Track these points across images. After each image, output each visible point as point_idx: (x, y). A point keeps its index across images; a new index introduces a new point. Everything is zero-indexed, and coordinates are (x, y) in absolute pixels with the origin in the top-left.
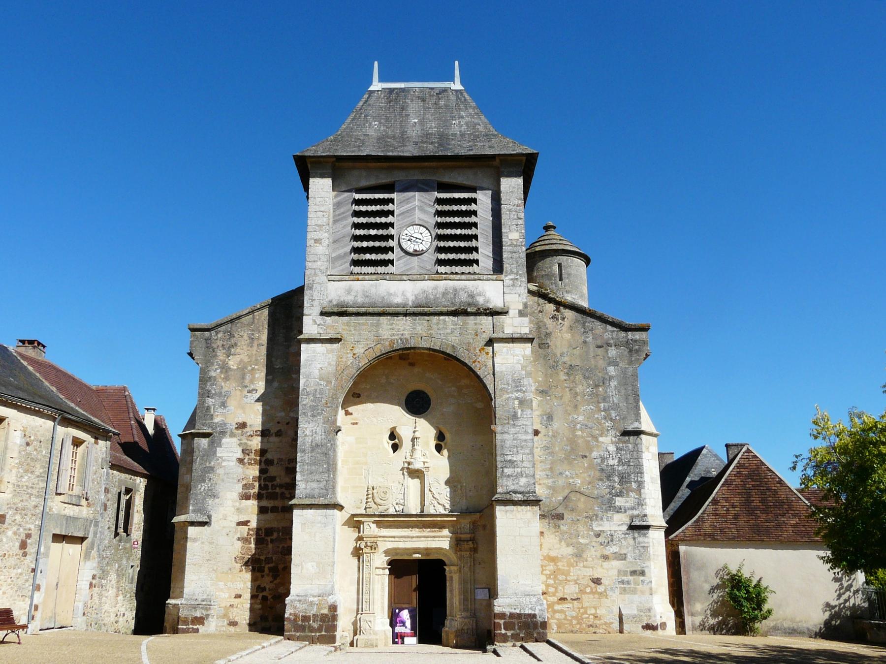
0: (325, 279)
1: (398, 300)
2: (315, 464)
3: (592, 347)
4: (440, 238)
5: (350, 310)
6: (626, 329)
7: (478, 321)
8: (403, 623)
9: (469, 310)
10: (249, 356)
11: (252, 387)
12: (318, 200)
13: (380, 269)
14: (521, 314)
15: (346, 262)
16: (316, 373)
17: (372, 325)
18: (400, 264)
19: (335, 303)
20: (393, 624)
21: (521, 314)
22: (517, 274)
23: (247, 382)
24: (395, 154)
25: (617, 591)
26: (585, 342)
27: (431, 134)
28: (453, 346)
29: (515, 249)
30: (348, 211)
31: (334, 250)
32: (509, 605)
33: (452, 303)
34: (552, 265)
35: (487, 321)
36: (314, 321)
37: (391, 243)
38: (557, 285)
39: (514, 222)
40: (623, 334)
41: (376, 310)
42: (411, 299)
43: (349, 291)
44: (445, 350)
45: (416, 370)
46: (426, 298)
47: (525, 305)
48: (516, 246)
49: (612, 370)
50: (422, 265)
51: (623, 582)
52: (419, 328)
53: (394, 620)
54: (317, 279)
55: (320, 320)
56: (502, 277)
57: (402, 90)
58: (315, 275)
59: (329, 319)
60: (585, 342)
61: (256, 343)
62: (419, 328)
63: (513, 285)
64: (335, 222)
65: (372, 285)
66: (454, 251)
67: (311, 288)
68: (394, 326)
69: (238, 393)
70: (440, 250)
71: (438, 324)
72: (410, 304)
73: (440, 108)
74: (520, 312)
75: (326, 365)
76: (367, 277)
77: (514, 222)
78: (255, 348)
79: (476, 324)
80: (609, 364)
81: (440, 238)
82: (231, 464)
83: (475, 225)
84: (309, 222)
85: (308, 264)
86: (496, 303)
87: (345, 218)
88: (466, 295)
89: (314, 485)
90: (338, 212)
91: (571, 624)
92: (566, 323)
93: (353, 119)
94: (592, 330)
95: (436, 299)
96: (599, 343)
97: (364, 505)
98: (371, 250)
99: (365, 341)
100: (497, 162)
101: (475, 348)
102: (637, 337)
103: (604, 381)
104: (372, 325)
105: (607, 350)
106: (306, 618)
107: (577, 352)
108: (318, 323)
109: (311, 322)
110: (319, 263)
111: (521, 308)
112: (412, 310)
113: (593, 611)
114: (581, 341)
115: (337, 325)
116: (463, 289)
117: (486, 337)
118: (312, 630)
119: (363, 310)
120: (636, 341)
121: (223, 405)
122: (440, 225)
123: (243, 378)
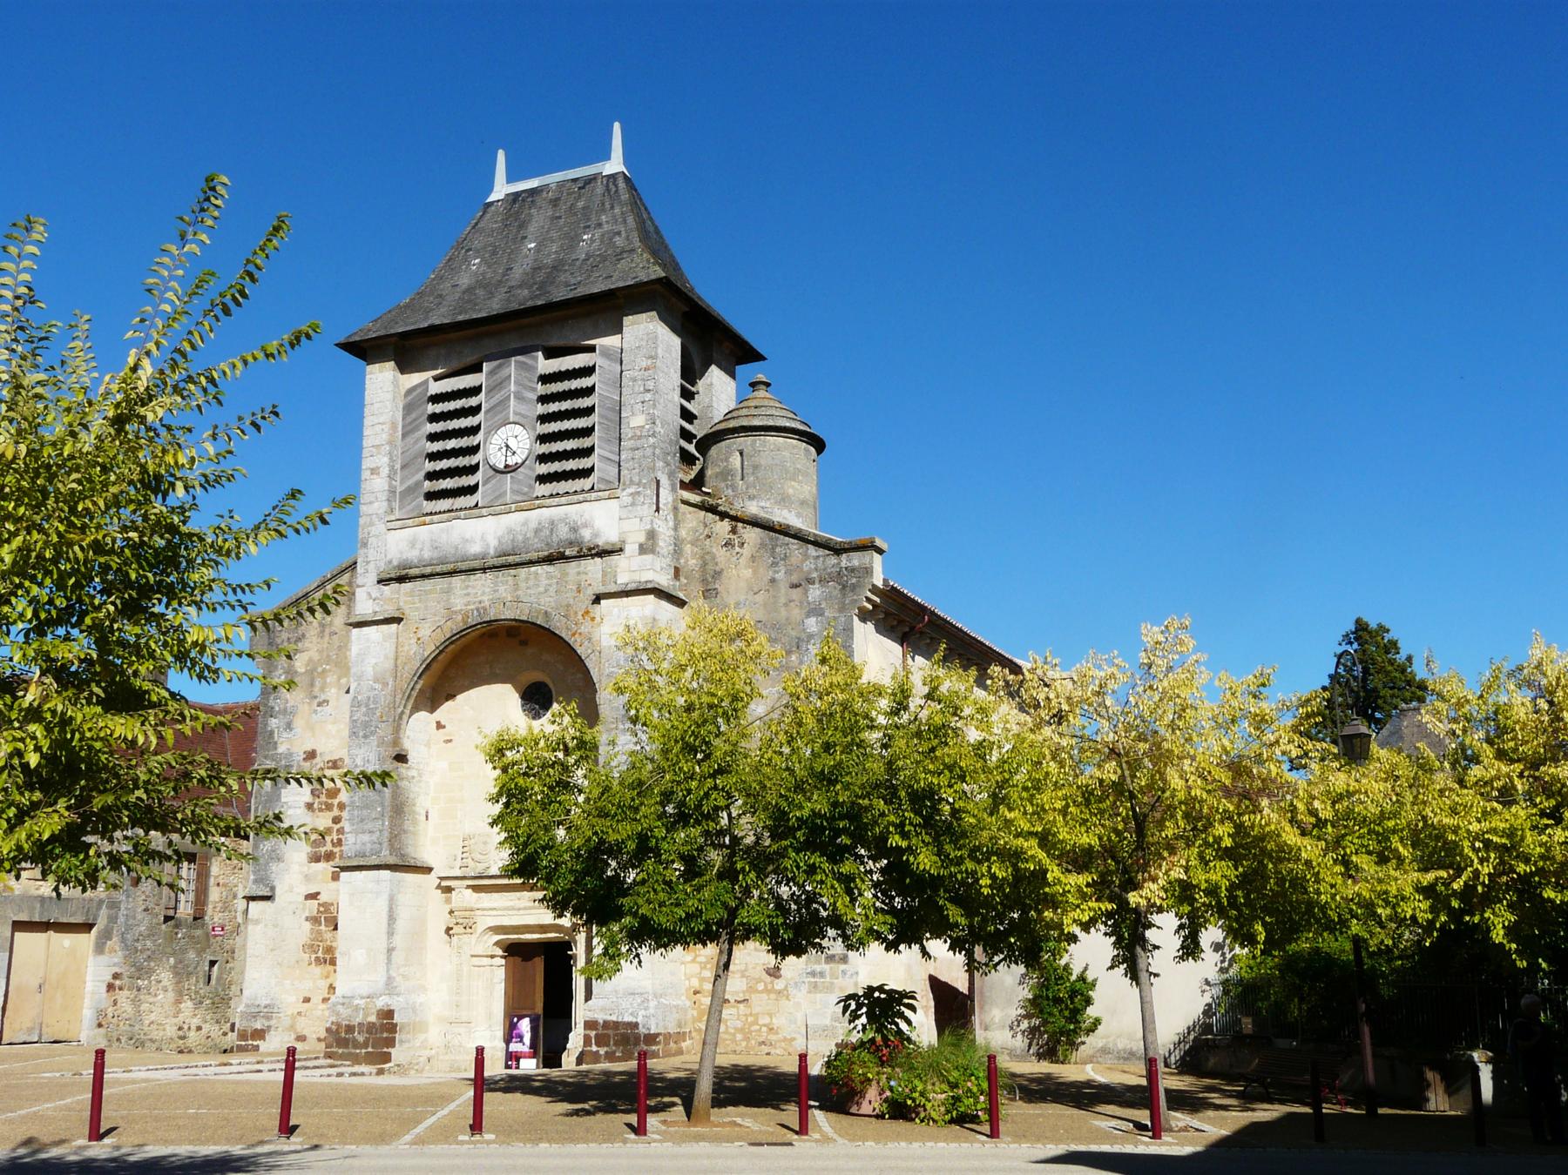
0: (382, 527)
1: (475, 549)
2: (366, 807)
3: (783, 587)
4: (544, 439)
6: (838, 550)
8: (521, 1037)
10: (320, 652)
11: (323, 697)
16: (370, 671)
17: (443, 591)
19: (395, 563)
20: (508, 1041)
23: (316, 690)
24: (467, 317)
25: (805, 988)
26: (773, 581)
32: (603, 1009)
34: (727, 455)
35: (594, 566)
38: (734, 487)
40: (833, 560)
41: (445, 568)
42: (492, 545)
43: (413, 544)
45: (530, 651)
48: (640, 438)
49: (812, 624)
51: (813, 974)
52: (502, 589)
53: (511, 1034)
55: (378, 590)
57: (533, 192)
58: (372, 524)
59: (387, 590)
60: (773, 581)
62: (502, 589)
63: (633, 504)
64: (404, 436)
66: (565, 459)
69: (306, 707)
71: (527, 579)
72: (492, 552)
74: (641, 546)
76: (435, 518)
78: (327, 638)
82: (299, 811)
85: (363, 508)
87: (417, 428)
88: (566, 529)
89: (366, 838)
90: (409, 419)
91: (734, 1041)
92: (746, 551)
94: (785, 557)
96: (795, 579)
97: (459, 863)
98: (450, 474)
102: (856, 563)
103: (798, 645)
104: (443, 591)
105: (806, 591)
106: (350, 1029)
107: (759, 598)
109: (364, 596)
111: (642, 539)
112: (491, 562)
113: (766, 1020)
117: (590, 593)
118: (356, 1045)
119: (428, 570)
120: (852, 570)
121: (289, 726)
123: (312, 685)
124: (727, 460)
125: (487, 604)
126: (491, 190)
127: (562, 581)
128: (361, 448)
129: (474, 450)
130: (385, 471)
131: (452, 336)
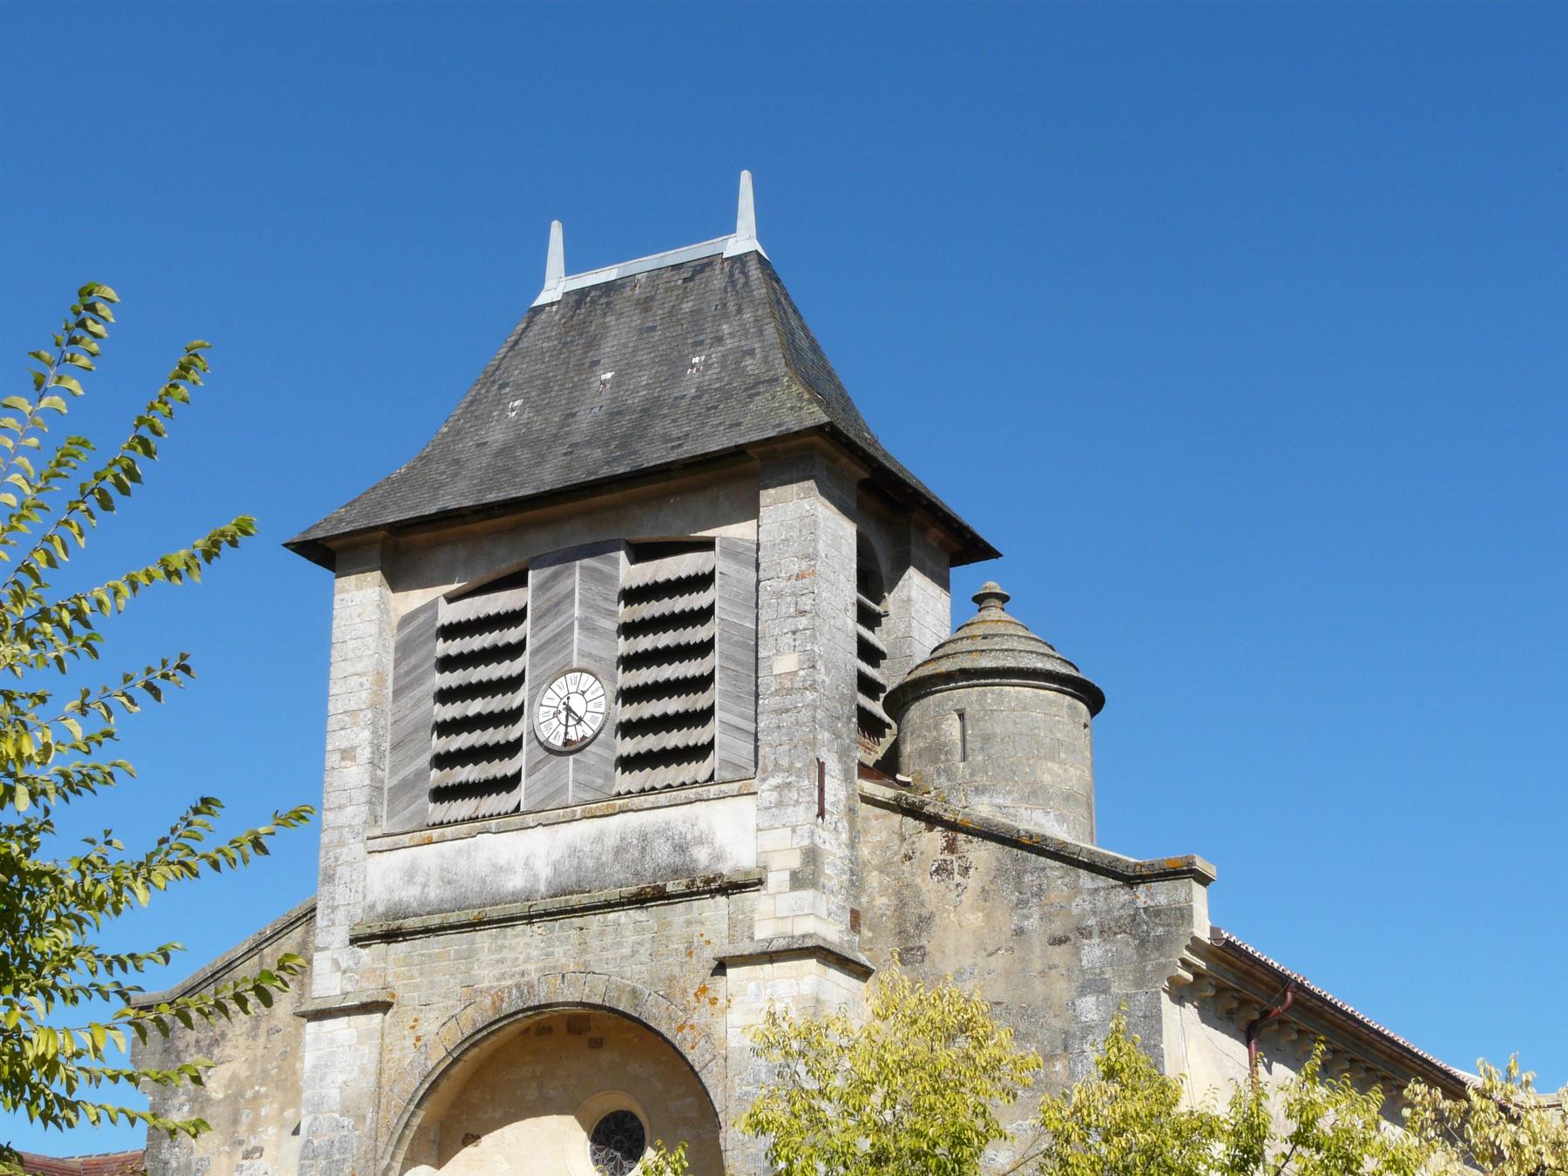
1: (515, 882)
3: (1038, 942)
4: (629, 696)
5: (411, 923)
6: (1131, 879)
7: (694, 915)
9: (670, 888)
10: (251, 1063)
11: (253, 1142)
12: (351, 644)
15: (417, 797)
16: (334, 1095)
17: (459, 956)
19: (380, 909)
22: (789, 771)
23: (242, 1130)
26: (1020, 932)
28: (634, 991)
29: (788, 701)
30: (426, 659)
33: (637, 873)
34: (937, 719)
36: (336, 962)
38: (949, 773)
40: (1122, 895)
43: (410, 875)
44: (613, 1004)
45: (606, 1057)
46: (578, 867)
48: (790, 691)
49: (1089, 1007)
52: (559, 951)
57: (608, 288)
58: (342, 843)
59: (365, 954)
60: (1020, 932)
61: (264, 1027)
63: (780, 804)
64: (397, 693)
65: (460, 851)
66: (665, 729)
68: (505, 953)
69: (224, 1160)
71: (602, 933)
72: (542, 887)
75: (355, 1074)
76: (448, 831)
77: (789, 625)
79: (689, 923)
80: (1083, 991)
84: (332, 708)
86: (738, 857)
87: (419, 681)
88: (668, 847)
90: (404, 667)
92: (973, 881)
94: (1040, 893)
95: (600, 867)
96: (1057, 928)
99: (450, 995)
101: (685, 991)
102: (1162, 900)
103: (1066, 1043)
105: (1077, 950)
107: (998, 962)
108: (344, 965)
110: (349, 810)
111: (795, 862)
112: (541, 906)
114: (1008, 930)
116: (664, 832)
117: (708, 956)
119: (436, 920)
120: (1157, 912)
123: (235, 1121)
124: (937, 726)
125: (534, 976)
126: (539, 286)
128: (324, 716)
129: (513, 716)
130: (365, 754)
131: (477, 527)
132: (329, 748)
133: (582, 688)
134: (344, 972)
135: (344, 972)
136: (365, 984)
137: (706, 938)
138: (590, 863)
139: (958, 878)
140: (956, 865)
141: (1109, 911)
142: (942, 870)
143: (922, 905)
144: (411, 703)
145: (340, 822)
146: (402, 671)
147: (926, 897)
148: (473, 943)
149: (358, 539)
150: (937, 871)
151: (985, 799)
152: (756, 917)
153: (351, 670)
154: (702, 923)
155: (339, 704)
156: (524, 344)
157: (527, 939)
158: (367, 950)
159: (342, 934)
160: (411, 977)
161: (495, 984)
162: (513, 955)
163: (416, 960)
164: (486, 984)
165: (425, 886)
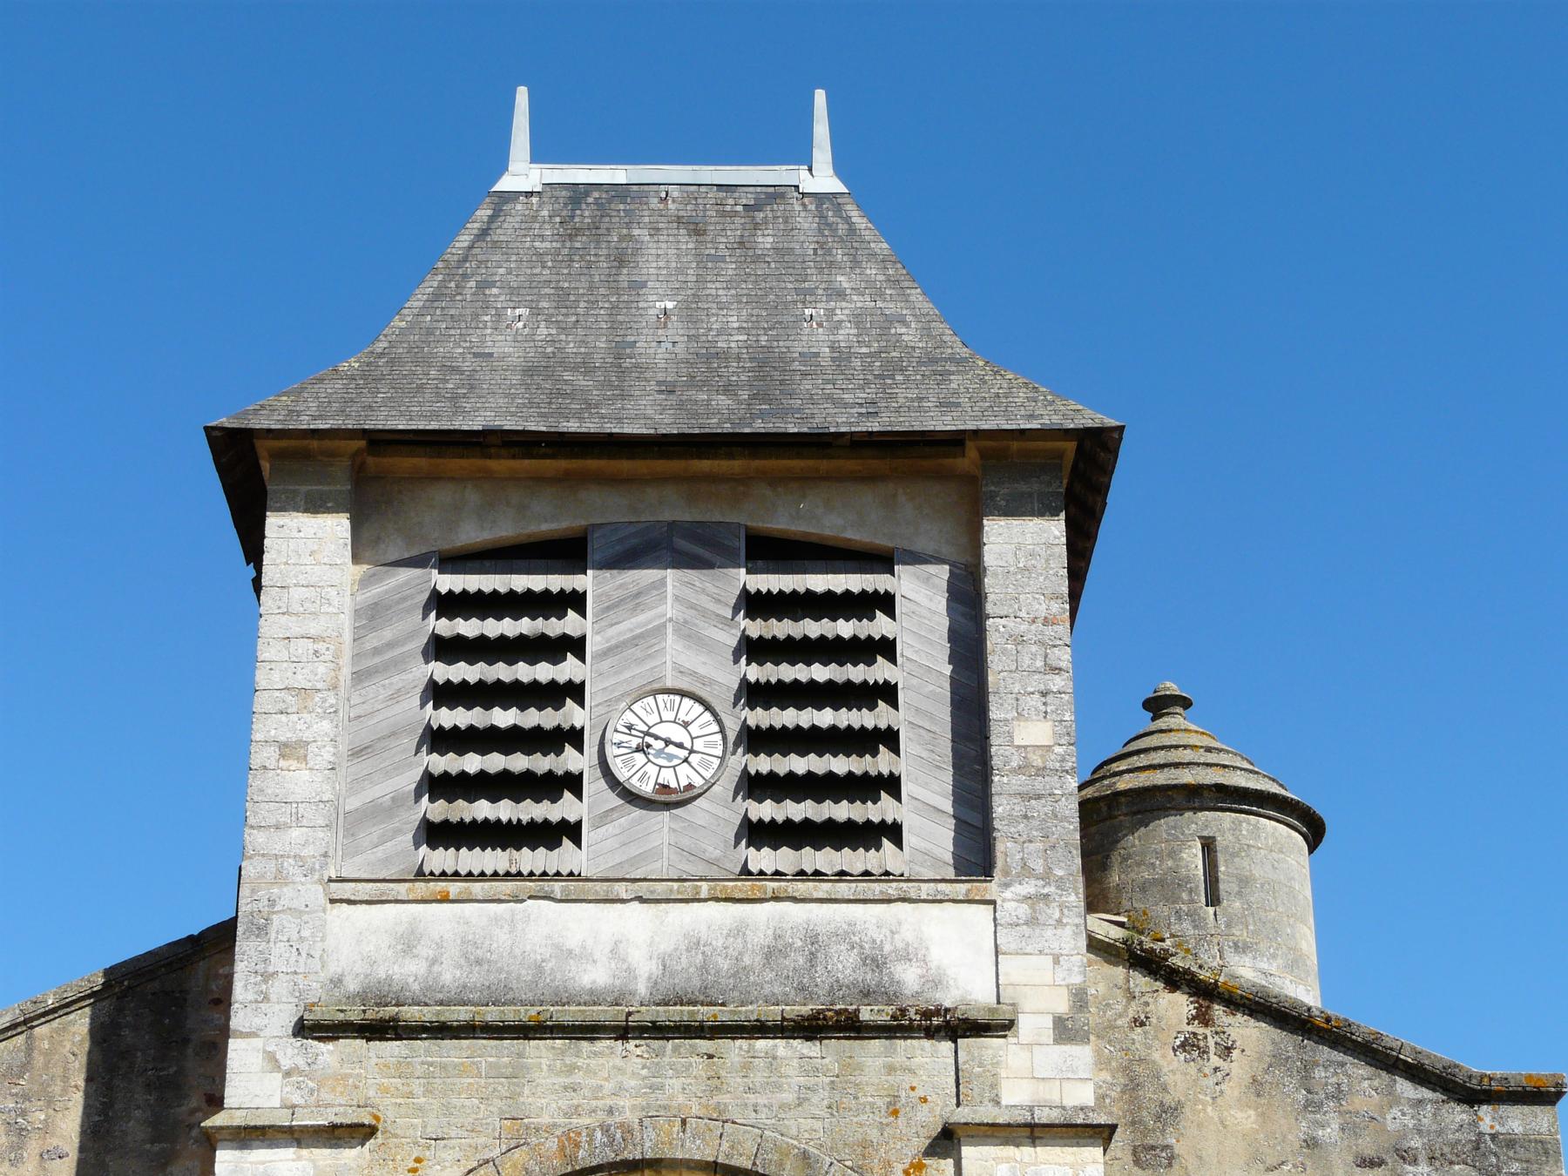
0: (315, 894)
1: (595, 976)
4: (755, 740)
5: (412, 1014)
6: (1471, 1094)
7: (899, 1059)
9: (866, 1015)
12: (297, 594)
13: (530, 859)
14: (1065, 1031)
15: (398, 832)
17: (496, 1073)
18: (608, 837)
19: (352, 986)
21: (1065, 1031)
22: (1046, 877)
26: (1311, 1143)
27: (723, 356)
28: (805, 1155)
29: (1039, 784)
30: (411, 636)
31: (355, 785)
33: (802, 988)
34: (1176, 844)
35: (930, 1059)
36: (272, 1060)
37: (570, 760)
38: (1198, 922)
39: (1036, 683)
40: (1458, 1114)
41: (511, 1014)
42: (644, 973)
43: (408, 943)
46: (704, 968)
47: (1080, 998)
48: (1041, 771)
50: (685, 842)
52: (674, 1084)
54: (286, 896)
55: (293, 1052)
56: (992, 889)
57: (619, 192)
58: (281, 879)
59: (328, 1053)
60: (1311, 1143)
61: (33, 1147)
62: (674, 1084)
63: (1032, 922)
64: (359, 677)
65: (496, 920)
67: (261, 931)
68: (578, 1077)
70: (755, 786)
71: (746, 1067)
72: (642, 989)
73: (757, 259)
76: (477, 888)
77: (1036, 683)
79: (891, 1069)
81: (755, 740)
83: (888, 692)
84: (262, 678)
85: (255, 839)
86: (969, 988)
87: (397, 664)
88: (852, 958)
90: (372, 641)
92: (1238, 1067)
93: (436, 297)
94: (1338, 1095)
95: (740, 972)
96: (1368, 1146)
98: (498, 783)
100: (968, 461)
104: (496, 1073)
108: (286, 1063)
110: (295, 833)
111: (1062, 1006)
112: (648, 1014)
115: (358, 1074)
116: (845, 936)
117: (929, 1120)
119: (461, 1014)
120: (1511, 1143)
122: (755, 694)
124: (1173, 854)
125: (632, 1118)
126: (502, 167)
127: (843, 1083)
130: (323, 755)
131: (501, 465)
132: (257, 736)
133: (682, 716)
134: (288, 1074)
135: (288, 1074)
136: (326, 1096)
137: (920, 1092)
138: (725, 965)
139: (1215, 1061)
140: (1211, 1042)
141: (1440, 1133)
142: (1189, 1045)
143: (1165, 1089)
144: (384, 694)
145: (277, 848)
146: (368, 646)
147: (1168, 1079)
148: (520, 1055)
149: (314, 444)
150: (1183, 1046)
151: (1247, 960)
152: (1003, 1075)
153: (296, 630)
154: (912, 1071)
155: (276, 676)
156: (498, 235)
157: (618, 1062)
158: (330, 1046)
159: (285, 1017)
160: (410, 1095)
161: (561, 1121)
162: (593, 1082)
163: (419, 1070)
164: (545, 1119)
165: (434, 962)
